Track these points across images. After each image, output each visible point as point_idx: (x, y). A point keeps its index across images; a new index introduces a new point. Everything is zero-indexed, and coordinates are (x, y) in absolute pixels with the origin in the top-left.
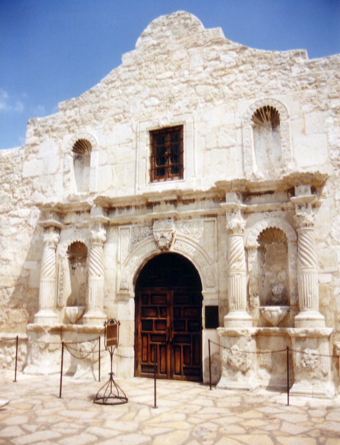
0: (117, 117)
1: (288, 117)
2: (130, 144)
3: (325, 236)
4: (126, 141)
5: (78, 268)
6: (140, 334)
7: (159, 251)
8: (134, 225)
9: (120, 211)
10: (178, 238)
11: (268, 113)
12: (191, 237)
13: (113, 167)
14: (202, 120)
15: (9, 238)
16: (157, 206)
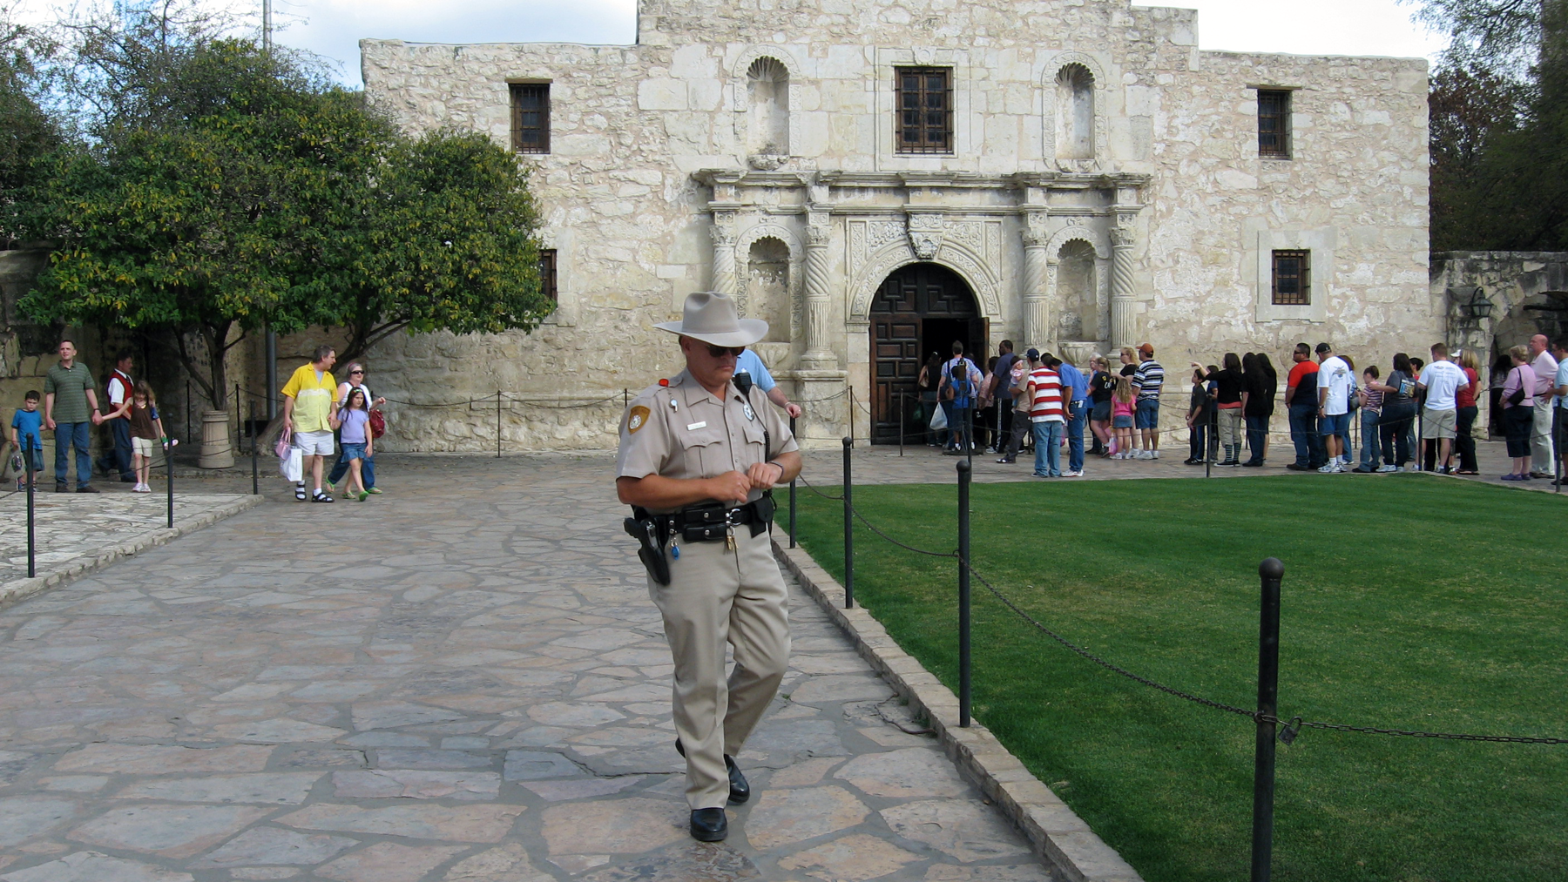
0: (836, 30)
1: (1105, 86)
2: (862, 83)
3: (1142, 255)
4: (856, 77)
5: (753, 279)
6: (874, 381)
7: (916, 261)
8: (872, 218)
9: (848, 193)
10: (945, 243)
11: (1073, 71)
12: (964, 244)
13: (833, 116)
14: (982, 66)
15: (618, 221)
16: (917, 194)
